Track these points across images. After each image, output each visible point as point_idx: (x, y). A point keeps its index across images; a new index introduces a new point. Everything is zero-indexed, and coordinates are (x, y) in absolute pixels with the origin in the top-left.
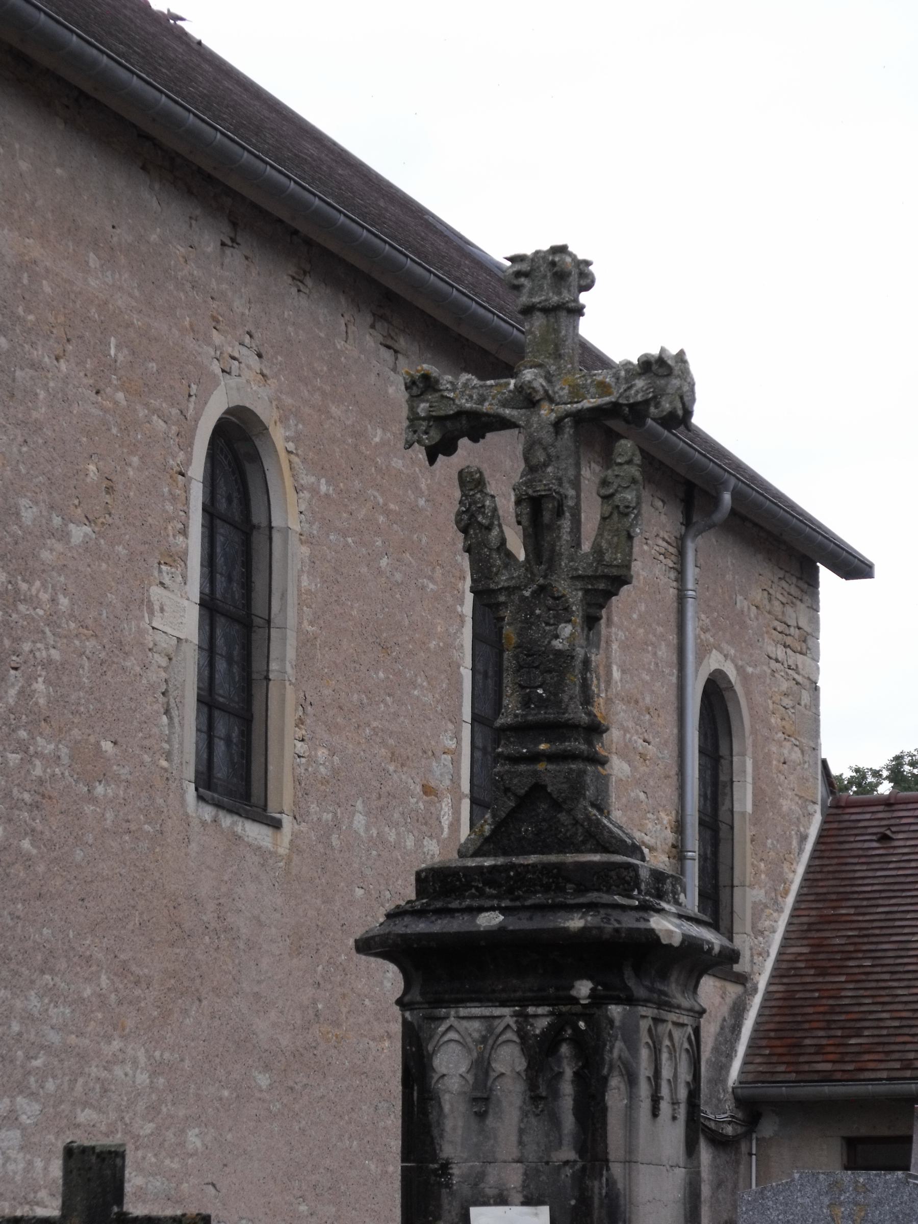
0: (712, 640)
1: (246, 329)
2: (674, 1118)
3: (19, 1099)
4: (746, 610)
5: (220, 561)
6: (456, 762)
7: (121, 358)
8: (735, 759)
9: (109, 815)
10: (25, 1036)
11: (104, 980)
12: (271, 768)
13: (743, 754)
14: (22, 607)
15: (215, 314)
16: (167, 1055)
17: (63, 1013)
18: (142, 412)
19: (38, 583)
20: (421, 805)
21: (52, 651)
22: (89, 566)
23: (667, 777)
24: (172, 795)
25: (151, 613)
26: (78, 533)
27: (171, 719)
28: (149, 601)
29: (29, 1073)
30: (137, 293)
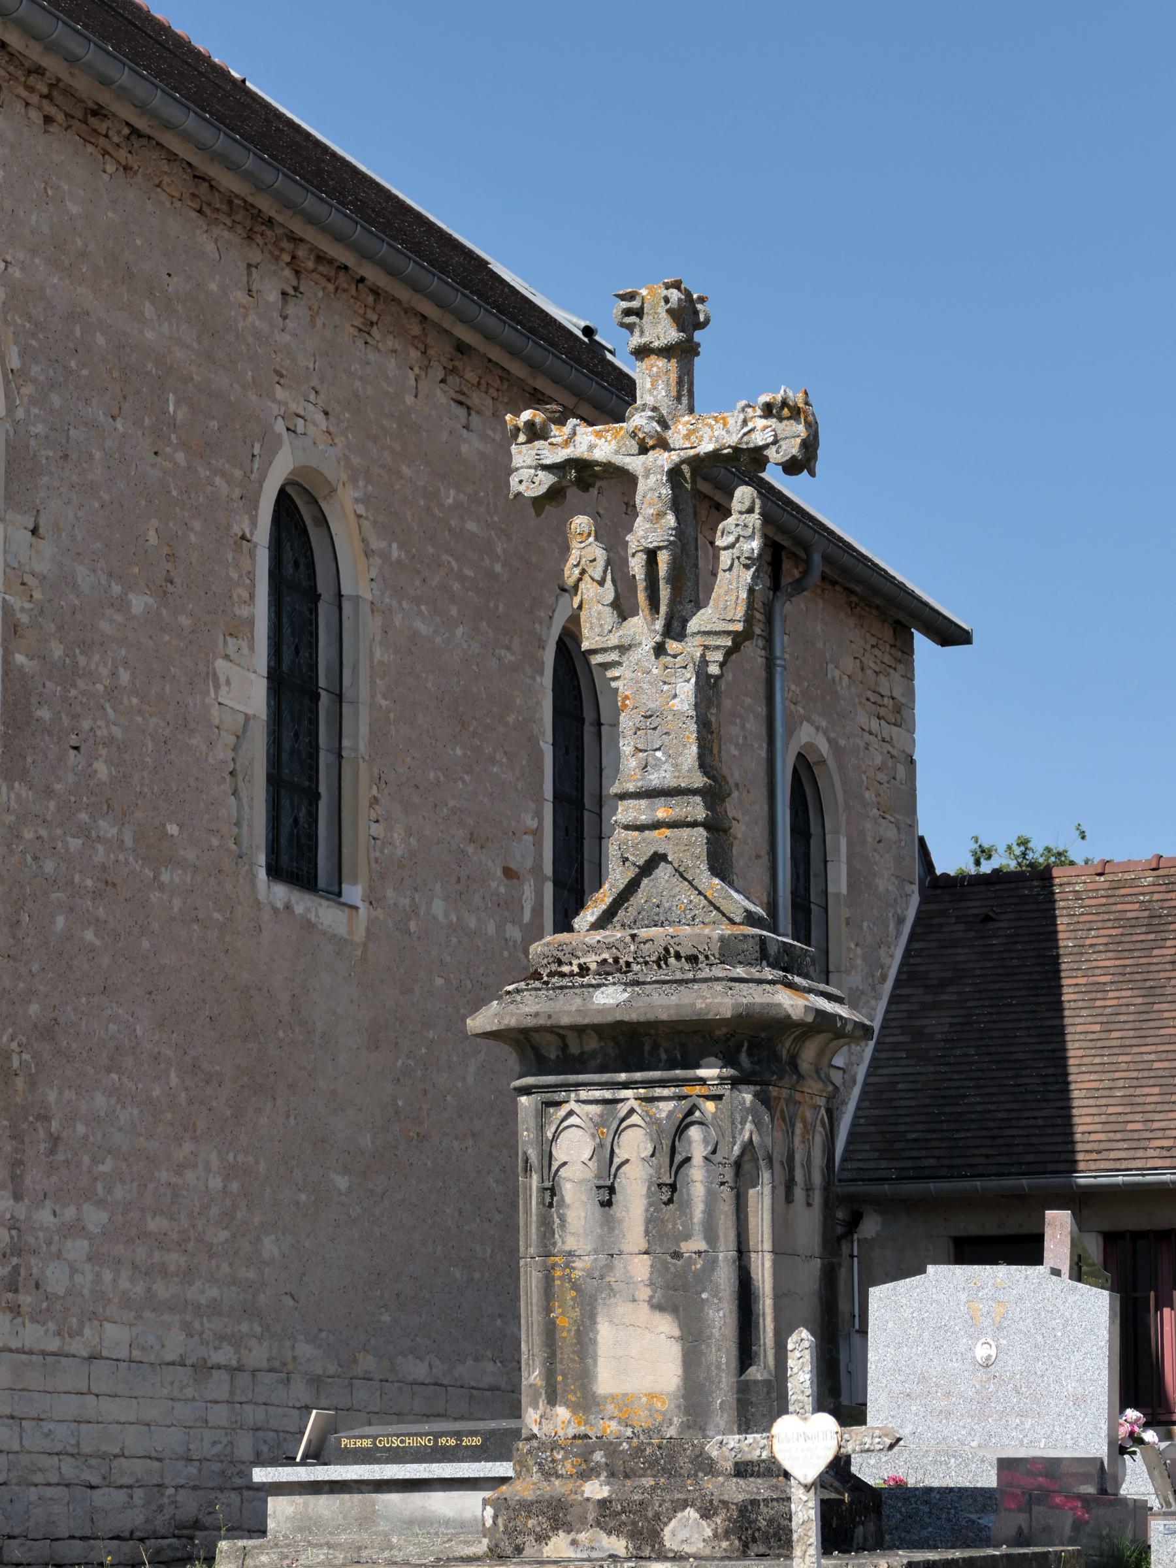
0: (802, 711)
1: (312, 384)
2: (809, 1205)
3: (87, 1207)
4: (837, 679)
5: (287, 631)
6: (538, 844)
7: (180, 415)
8: (828, 837)
9: (177, 903)
10: (91, 1139)
11: (174, 1080)
12: (344, 850)
13: (837, 832)
14: (81, 684)
15: (278, 368)
16: (241, 1158)
17: (131, 1114)
18: (203, 473)
19: (97, 657)
20: (502, 890)
21: (113, 728)
22: (151, 637)
23: (758, 857)
24: (242, 881)
25: (217, 687)
26: (139, 603)
27: (239, 799)
28: (215, 675)
29: (96, 1179)
30: (195, 345)
